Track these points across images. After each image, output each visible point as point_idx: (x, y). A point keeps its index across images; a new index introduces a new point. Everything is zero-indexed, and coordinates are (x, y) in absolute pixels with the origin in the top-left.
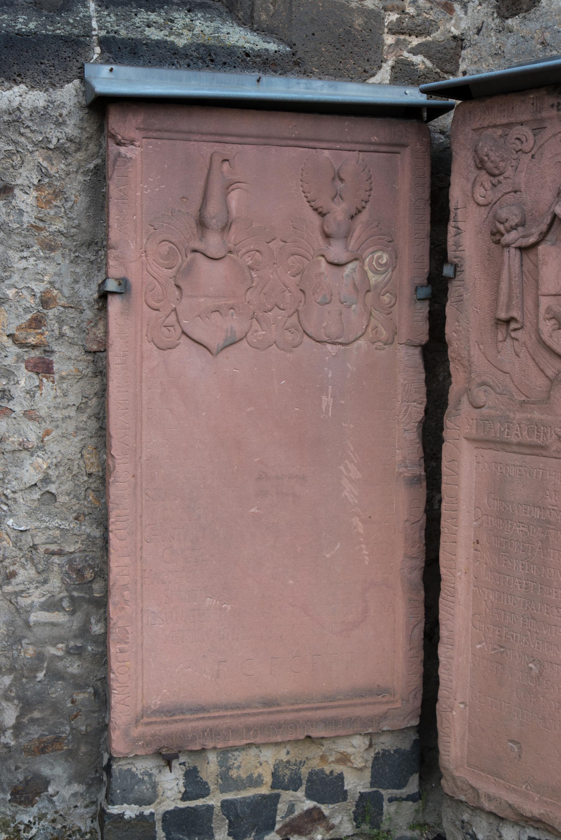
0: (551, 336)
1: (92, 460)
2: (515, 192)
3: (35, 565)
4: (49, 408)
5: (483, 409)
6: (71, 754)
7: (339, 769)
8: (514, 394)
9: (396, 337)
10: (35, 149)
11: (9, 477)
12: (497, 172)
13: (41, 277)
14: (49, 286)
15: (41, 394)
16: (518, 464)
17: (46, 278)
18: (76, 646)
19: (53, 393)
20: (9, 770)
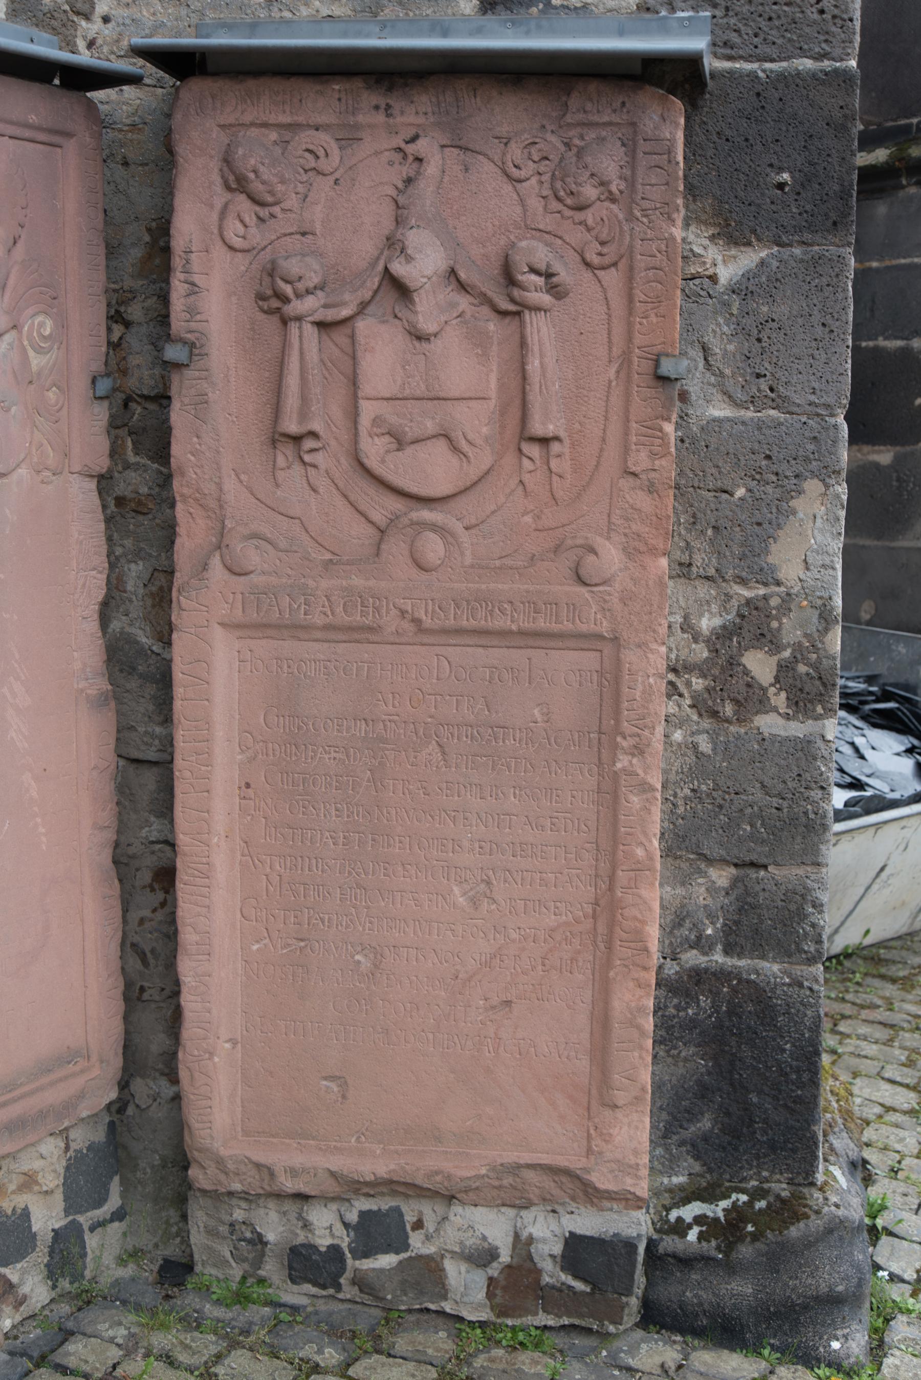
0: (383, 461)
2: (304, 234)
5: (252, 576)
7: (21, 1200)
12: (270, 199)
16: (322, 657)
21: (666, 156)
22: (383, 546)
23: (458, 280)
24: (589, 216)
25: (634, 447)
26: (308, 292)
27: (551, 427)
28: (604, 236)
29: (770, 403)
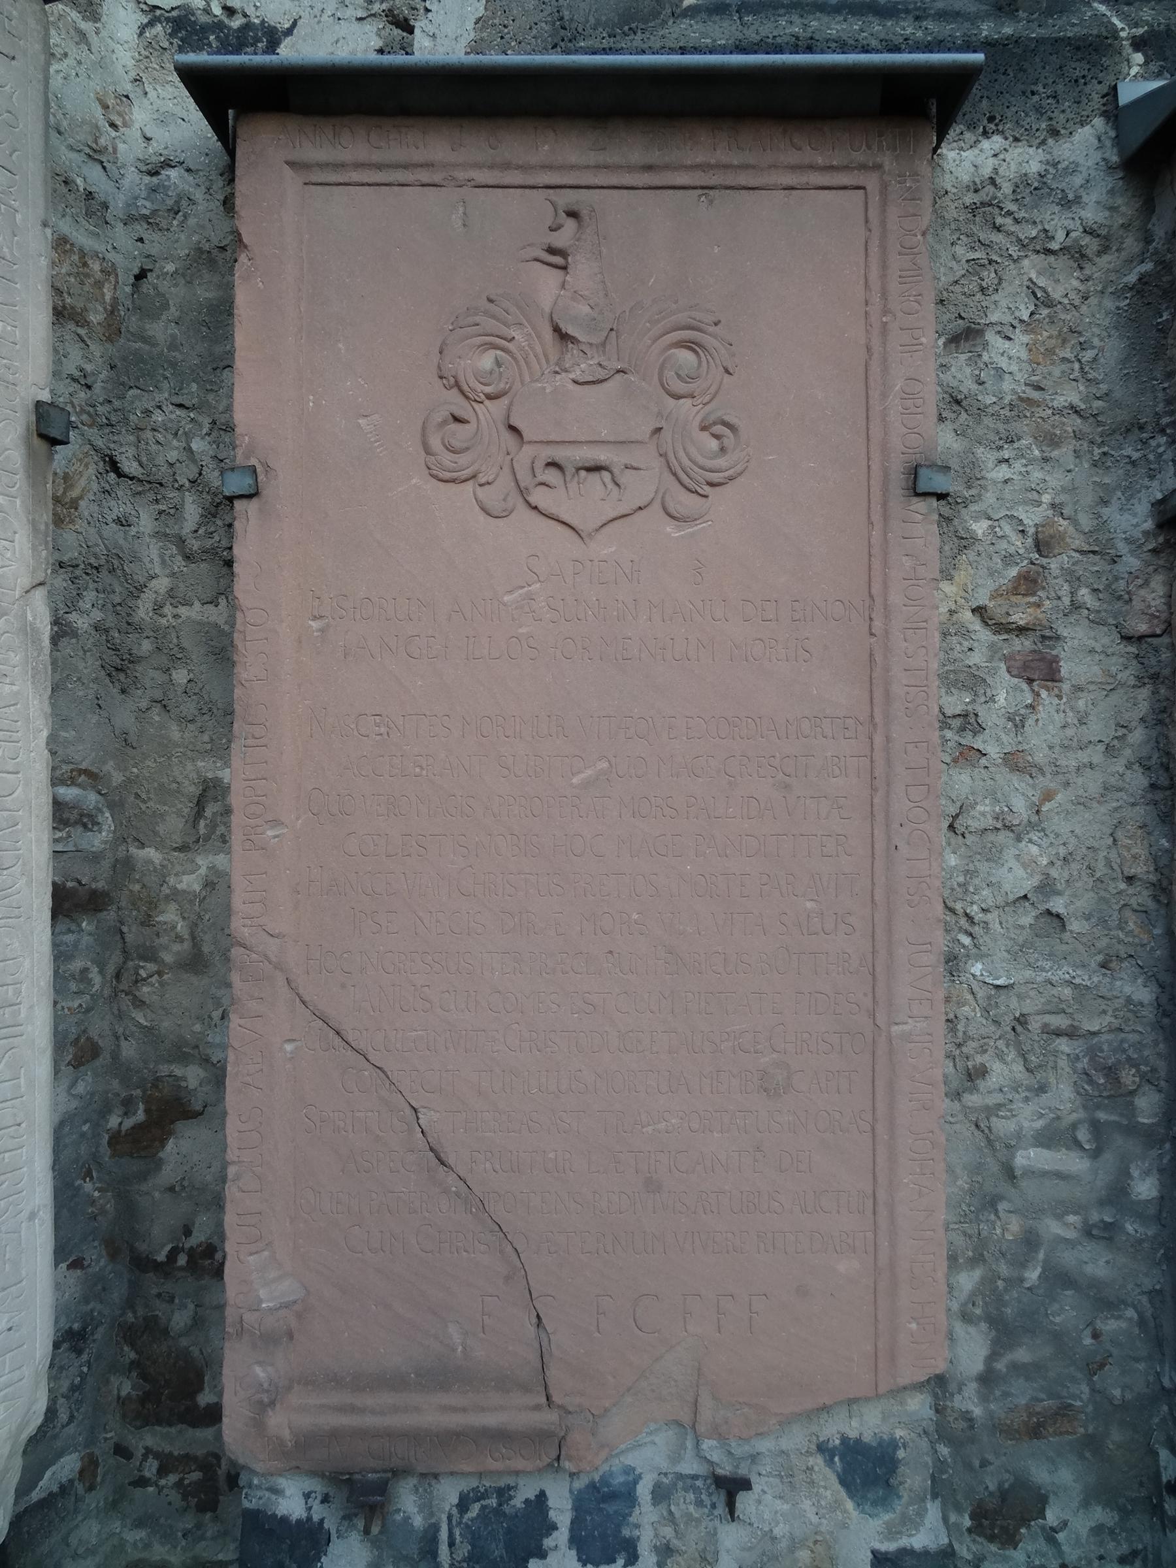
1: (1134, 851)
3: (1024, 1056)
4: (1050, 748)
6: (1092, 1444)
10: (1022, 254)
11: (976, 881)
13: (1035, 495)
14: (1050, 513)
15: (1037, 720)
17: (1046, 498)
18: (1102, 1221)
19: (1059, 718)
20: (968, 1466)
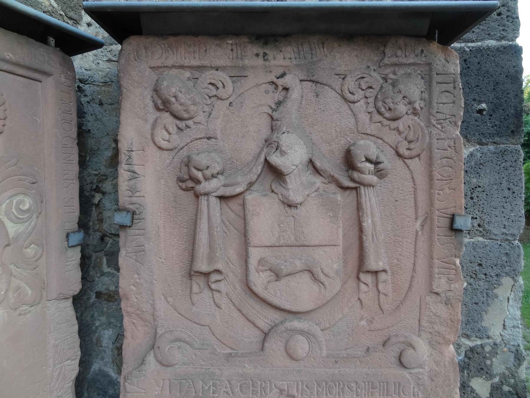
0: (266, 288)
2: (209, 138)
8: (216, 347)
9: (44, 293)
12: (186, 116)
21: (452, 84)
22: (266, 345)
23: (315, 167)
24: (400, 124)
25: (437, 276)
26: (213, 176)
27: (381, 264)
28: (411, 137)
29: (479, 234)
